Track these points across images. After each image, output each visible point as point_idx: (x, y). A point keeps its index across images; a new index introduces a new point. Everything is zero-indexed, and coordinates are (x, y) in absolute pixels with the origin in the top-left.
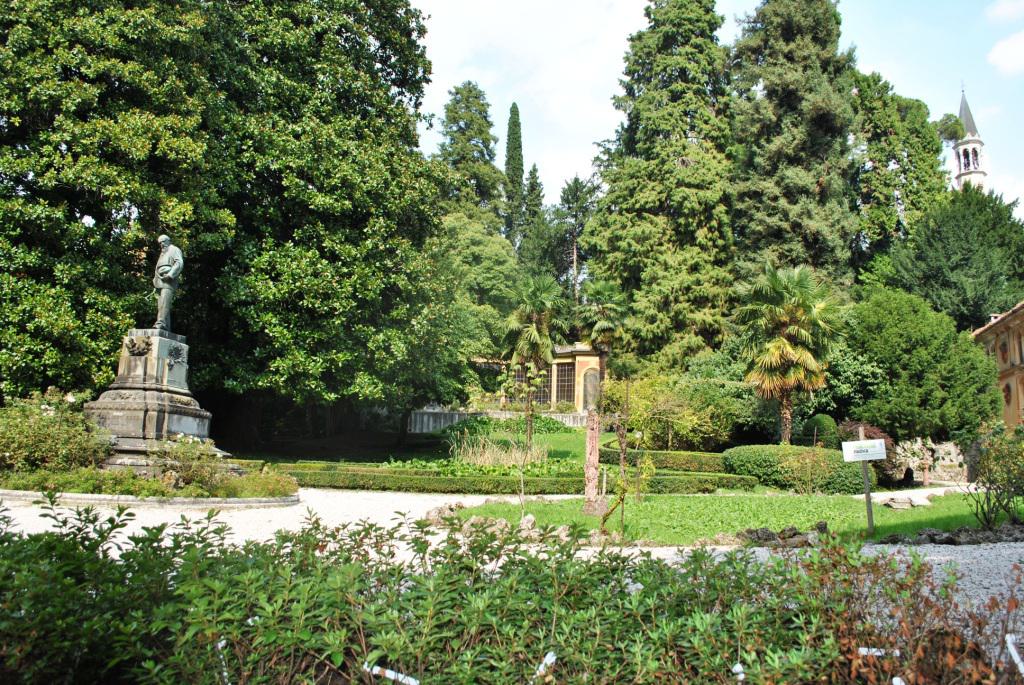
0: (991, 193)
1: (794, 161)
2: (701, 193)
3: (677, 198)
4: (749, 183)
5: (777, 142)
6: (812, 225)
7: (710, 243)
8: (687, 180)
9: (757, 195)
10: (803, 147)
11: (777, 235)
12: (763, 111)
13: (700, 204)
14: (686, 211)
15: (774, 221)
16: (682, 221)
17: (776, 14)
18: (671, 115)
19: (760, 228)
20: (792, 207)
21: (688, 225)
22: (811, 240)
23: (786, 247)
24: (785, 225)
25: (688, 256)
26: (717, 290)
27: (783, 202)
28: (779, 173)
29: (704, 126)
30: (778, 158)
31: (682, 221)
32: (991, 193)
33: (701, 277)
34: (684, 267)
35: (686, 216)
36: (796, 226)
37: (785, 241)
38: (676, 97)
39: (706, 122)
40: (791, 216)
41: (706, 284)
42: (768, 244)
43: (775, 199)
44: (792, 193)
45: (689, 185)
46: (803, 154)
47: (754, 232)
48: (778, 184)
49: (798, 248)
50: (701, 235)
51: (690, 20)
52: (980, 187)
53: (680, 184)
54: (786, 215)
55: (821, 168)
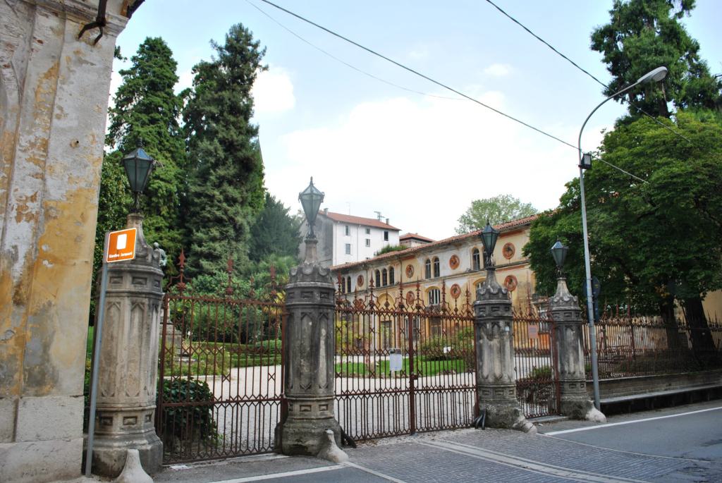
0: (280, 202)
1: (230, 183)
2: (169, 186)
3: (155, 186)
4: (203, 189)
5: (221, 172)
6: (239, 219)
7: (168, 216)
8: (161, 177)
9: (211, 198)
10: (234, 176)
11: (219, 222)
12: (219, 152)
13: (166, 191)
14: (160, 195)
15: (219, 214)
16: (154, 199)
17: (229, 99)
18: (150, 132)
19: (209, 216)
20: (229, 208)
21: (158, 203)
22: (237, 228)
23: (225, 229)
24: (225, 217)
25: (155, 221)
26: (171, 244)
27: (225, 205)
28: (224, 188)
29: (166, 143)
30: (222, 179)
31: (154, 199)
32: (280, 202)
33: (163, 235)
34: (152, 228)
35: (158, 197)
36: (231, 219)
37: (225, 226)
38: (153, 121)
39: (167, 141)
40: (229, 212)
41: (165, 240)
42: (213, 226)
43: (220, 202)
44: (231, 201)
45: (162, 180)
46: (234, 180)
47: (204, 217)
48: (221, 193)
49: (232, 232)
50: (164, 211)
51: (166, 77)
52: (274, 197)
53: (157, 177)
54: (226, 212)
55: (243, 189)
